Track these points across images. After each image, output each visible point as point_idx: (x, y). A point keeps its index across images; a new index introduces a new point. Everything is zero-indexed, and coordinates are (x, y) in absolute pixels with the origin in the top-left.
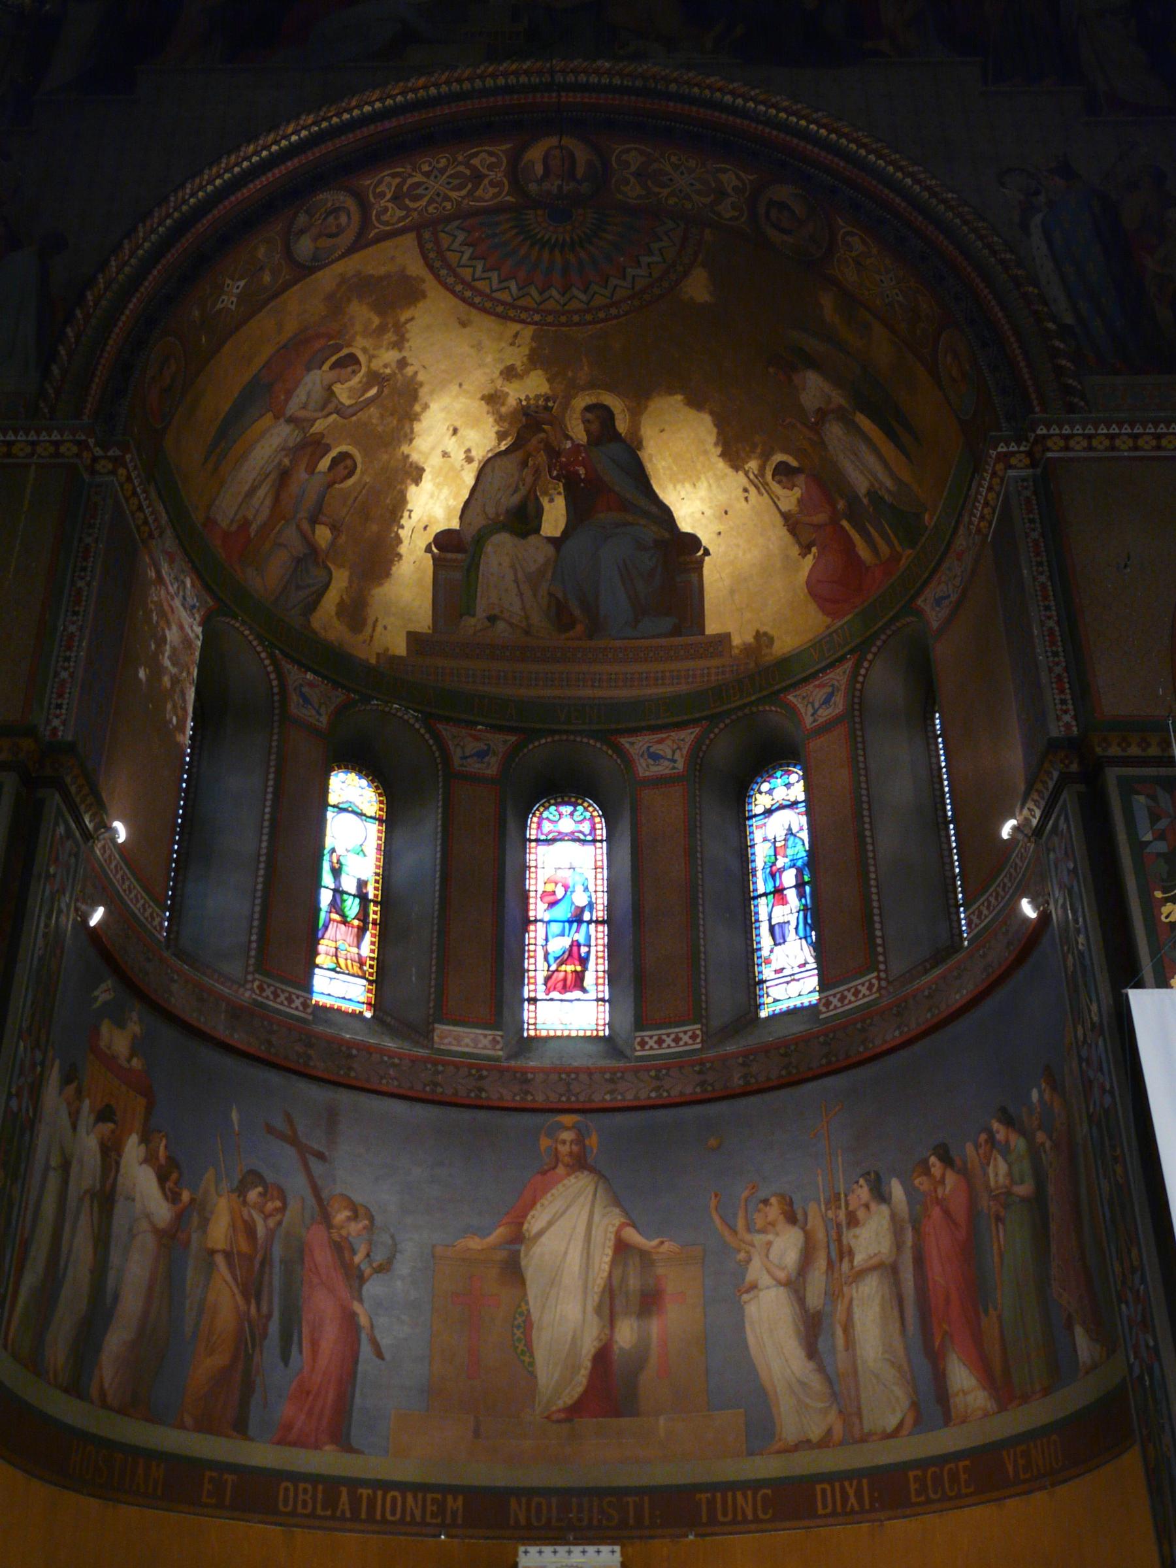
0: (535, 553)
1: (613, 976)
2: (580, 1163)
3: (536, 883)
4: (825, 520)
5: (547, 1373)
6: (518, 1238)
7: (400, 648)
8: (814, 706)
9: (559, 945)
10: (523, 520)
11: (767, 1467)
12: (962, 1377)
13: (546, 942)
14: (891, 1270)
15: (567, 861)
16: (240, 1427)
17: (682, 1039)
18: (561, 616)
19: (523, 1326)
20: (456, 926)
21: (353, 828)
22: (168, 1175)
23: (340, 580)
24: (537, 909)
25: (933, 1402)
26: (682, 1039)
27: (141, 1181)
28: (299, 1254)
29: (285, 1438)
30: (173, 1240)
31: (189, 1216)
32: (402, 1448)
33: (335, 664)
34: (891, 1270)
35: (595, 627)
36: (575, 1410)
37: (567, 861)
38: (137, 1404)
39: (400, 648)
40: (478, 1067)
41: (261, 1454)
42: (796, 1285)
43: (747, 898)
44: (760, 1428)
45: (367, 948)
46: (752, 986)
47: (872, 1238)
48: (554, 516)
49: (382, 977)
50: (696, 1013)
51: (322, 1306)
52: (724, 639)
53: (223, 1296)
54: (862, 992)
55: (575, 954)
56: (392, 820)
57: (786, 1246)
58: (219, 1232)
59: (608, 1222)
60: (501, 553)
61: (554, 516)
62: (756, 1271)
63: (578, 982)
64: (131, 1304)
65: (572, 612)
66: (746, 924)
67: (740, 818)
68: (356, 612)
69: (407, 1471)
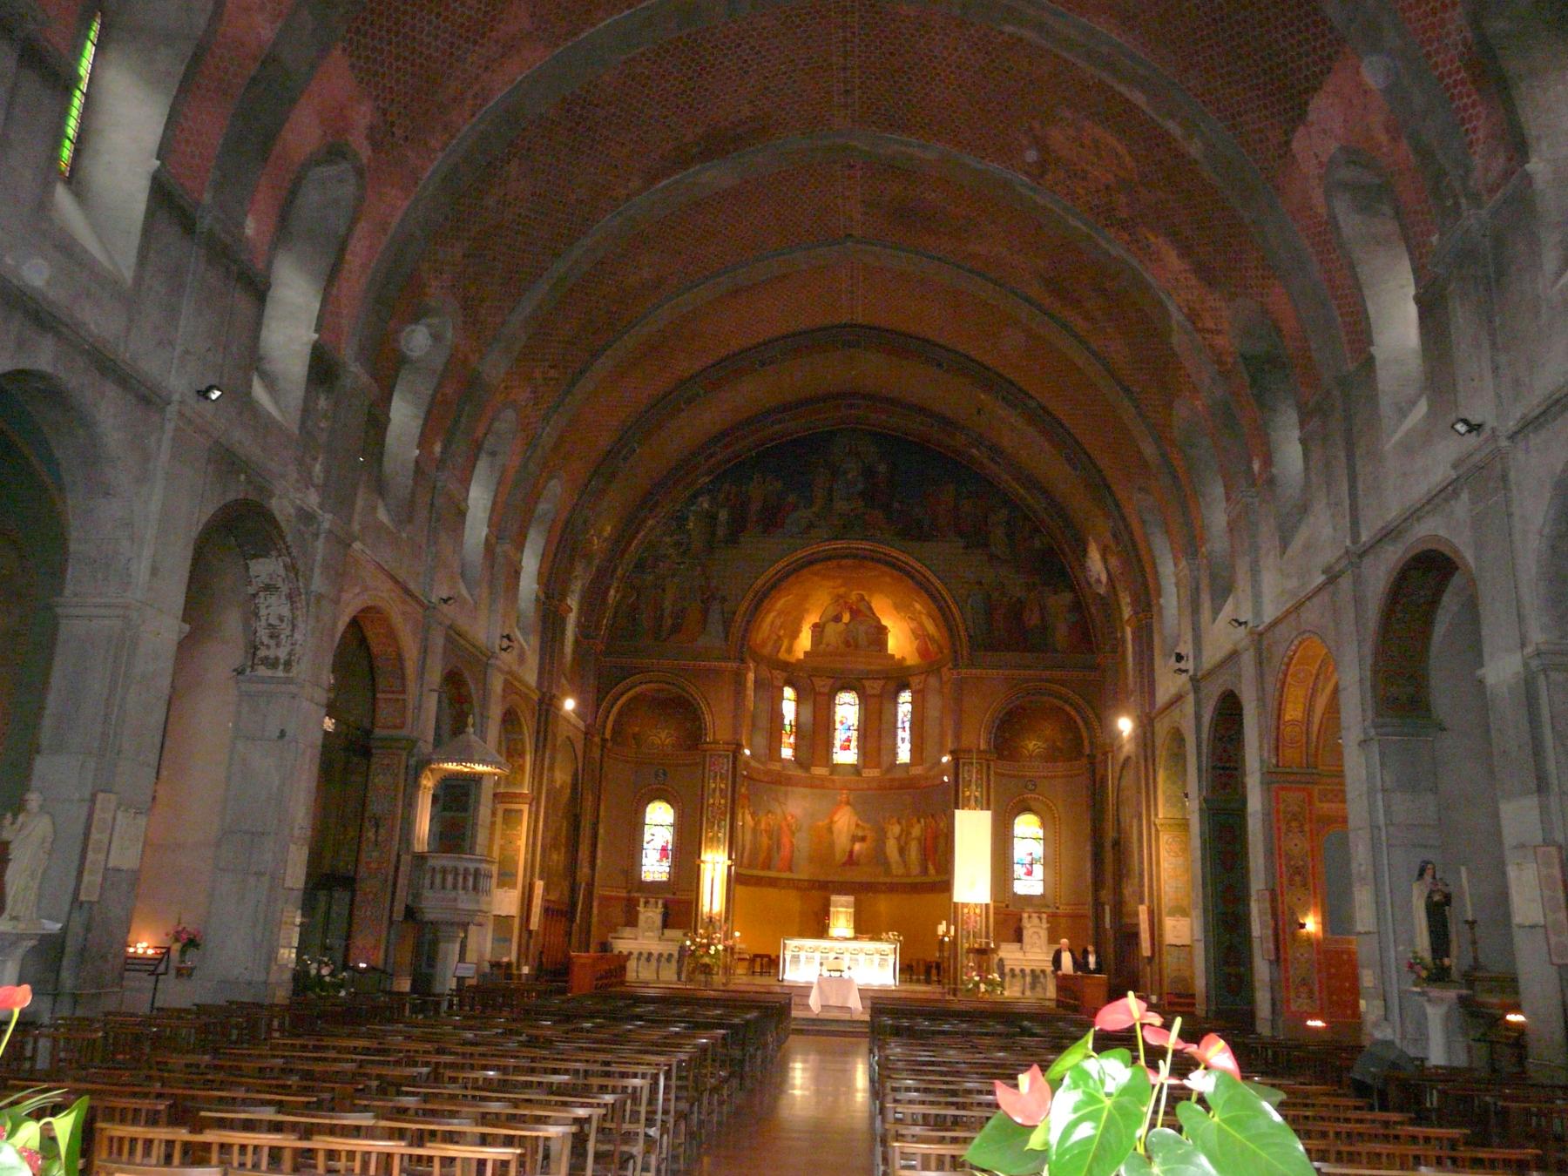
0: (841, 626)
1: (858, 747)
2: (848, 803)
3: (838, 718)
4: (920, 635)
5: (838, 857)
6: (832, 822)
7: (802, 656)
8: (915, 681)
9: (844, 737)
10: (837, 619)
11: (888, 880)
12: (931, 867)
13: (840, 736)
14: (919, 840)
15: (847, 709)
16: (769, 868)
17: (875, 773)
18: (848, 644)
19: (832, 845)
20: (817, 733)
21: (789, 709)
22: (753, 815)
23: (785, 643)
24: (838, 725)
25: (925, 871)
26: (875, 773)
27: (748, 818)
28: (780, 828)
29: (780, 871)
30: (754, 830)
31: (757, 823)
32: (803, 873)
33: (786, 666)
34: (919, 840)
35: (857, 647)
36: (844, 864)
37: (847, 709)
38: (750, 866)
39: (802, 656)
40: (822, 779)
41: (773, 874)
42: (898, 839)
43: (896, 728)
44: (888, 872)
45: (792, 740)
46: (895, 754)
47: (916, 831)
48: (846, 618)
49: (796, 748)
50: (878, 766)
51: (785, 840)
52: (892, 656)
53: (765, 840)
54: (917, 771)
55: (848, 740)
56: (798, 701)
57: (896, 829)
58: (763, 826)
59: (854, 819)
60: (832, 630)
61: (846, 618)
62: (889, 834)
63: (848, 748)
64: (748, 846)
65: (850, 643)
66: (895, 736)
67: (896, 703)
68: (790, 650)
69: (801, 877)
